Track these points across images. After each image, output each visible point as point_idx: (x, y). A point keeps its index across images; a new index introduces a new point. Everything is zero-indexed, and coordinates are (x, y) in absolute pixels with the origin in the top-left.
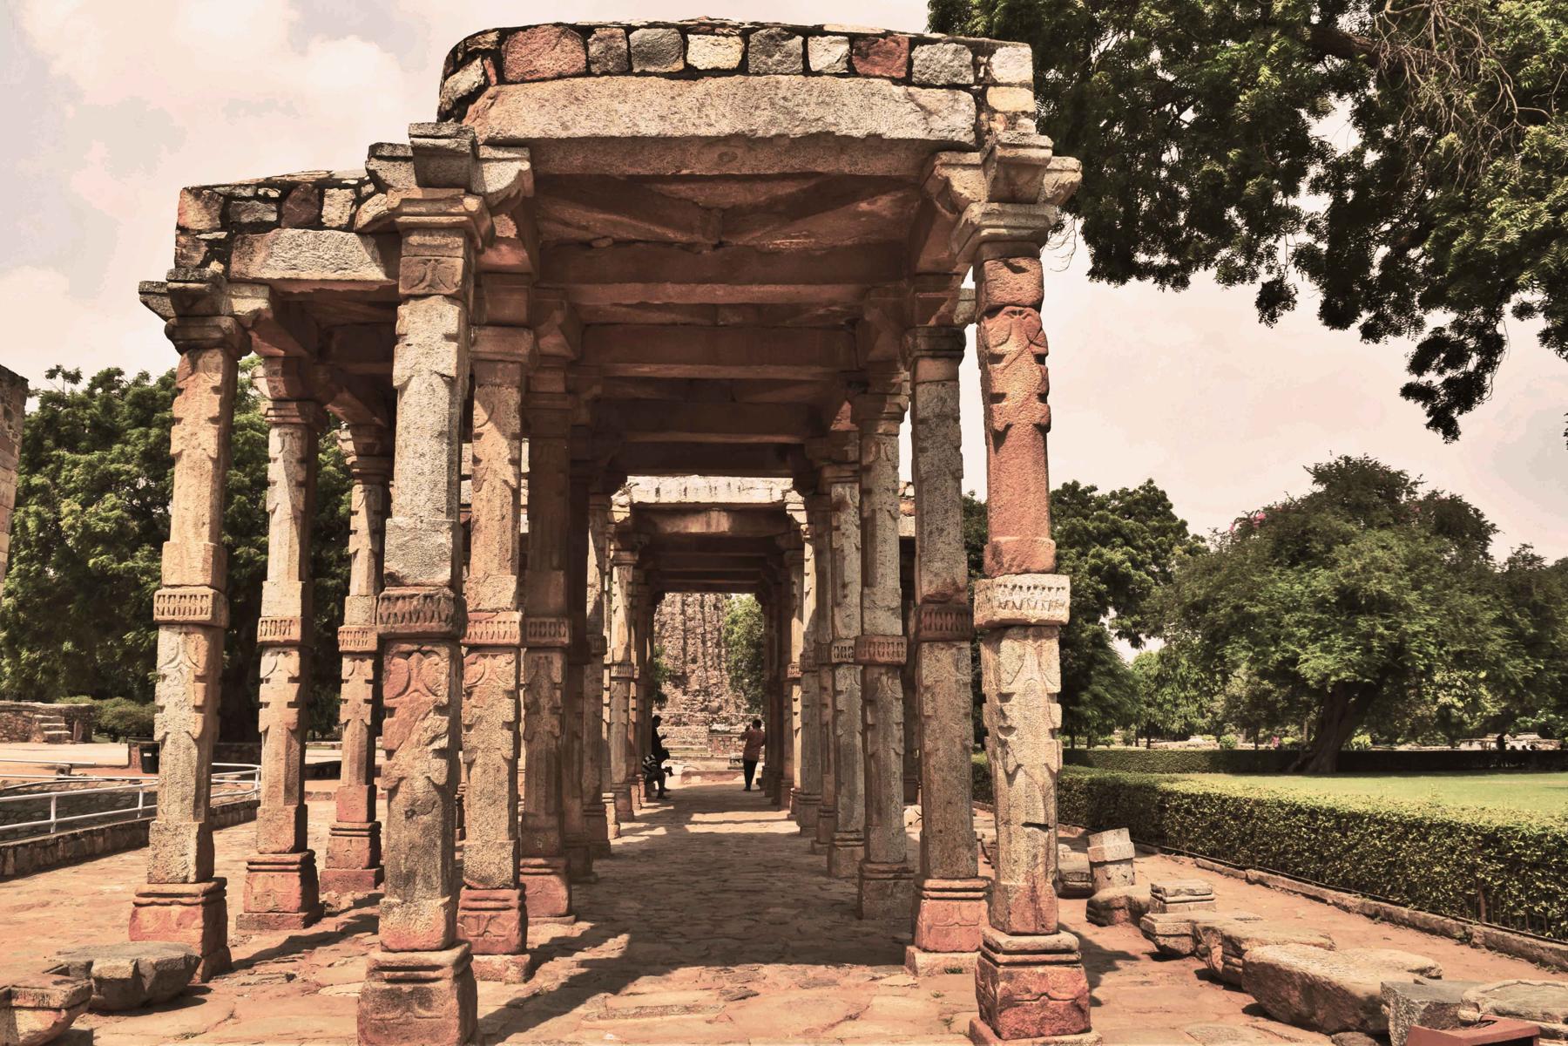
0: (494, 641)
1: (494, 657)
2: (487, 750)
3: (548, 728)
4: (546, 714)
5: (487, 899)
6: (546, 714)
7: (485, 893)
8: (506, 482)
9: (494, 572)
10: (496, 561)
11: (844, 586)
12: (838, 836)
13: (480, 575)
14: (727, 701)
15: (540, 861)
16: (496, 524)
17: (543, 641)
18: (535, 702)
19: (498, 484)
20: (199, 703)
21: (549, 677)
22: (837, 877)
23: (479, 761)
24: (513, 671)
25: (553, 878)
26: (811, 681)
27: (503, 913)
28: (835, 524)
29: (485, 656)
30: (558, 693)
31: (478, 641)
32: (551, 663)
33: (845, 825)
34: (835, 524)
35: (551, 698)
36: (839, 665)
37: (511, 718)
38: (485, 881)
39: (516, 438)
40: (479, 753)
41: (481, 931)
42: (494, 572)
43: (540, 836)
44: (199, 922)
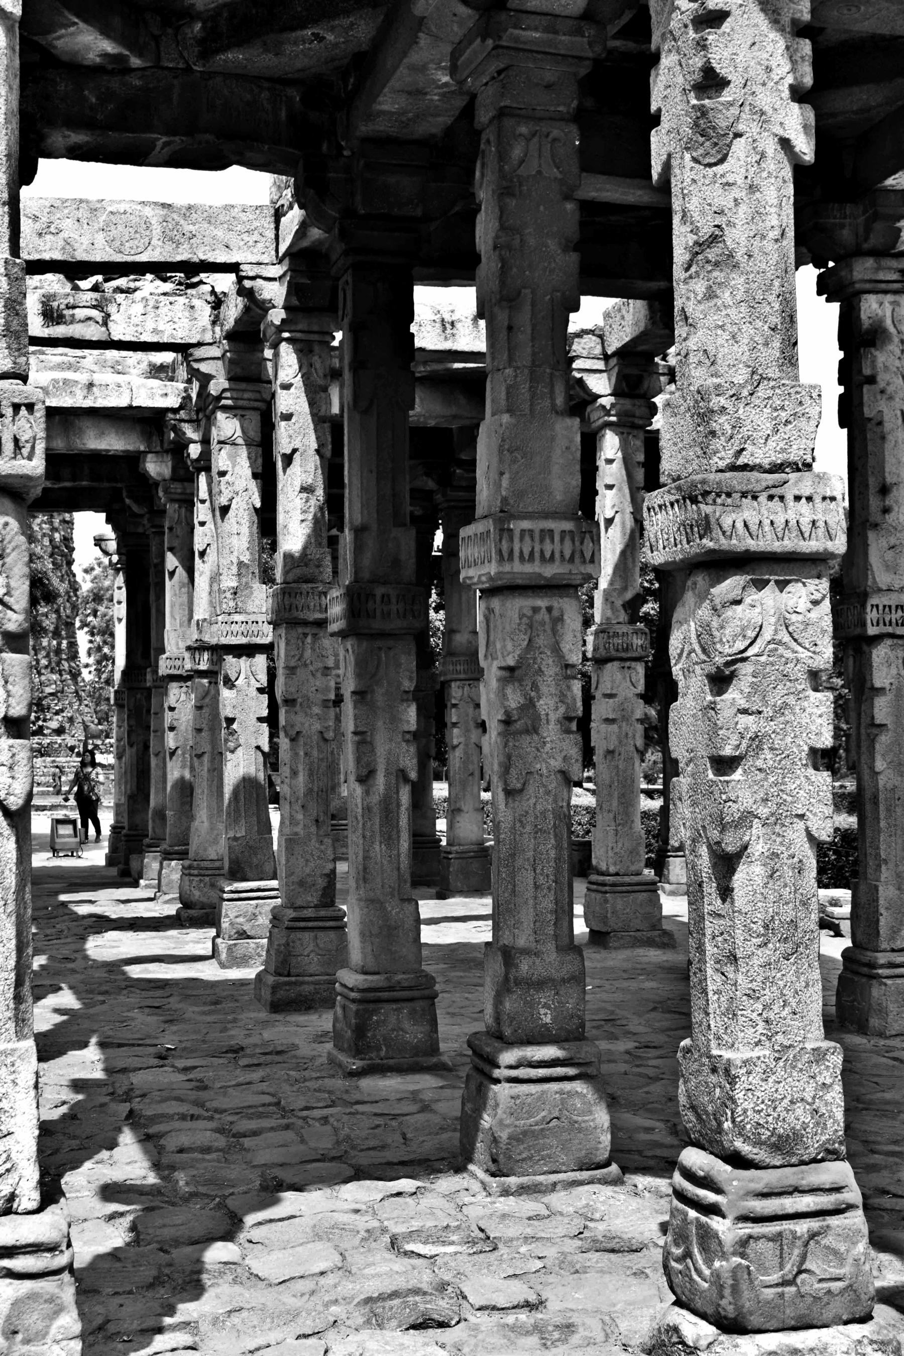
0: (789, 544)
1: (782, 585)
2: (775, 821)
3: (556, 763)
4: (551, 731)
5: (797, 1190)
6: (551, 731)
7: (789, 1176)
8: (785, 143)
9: (773, 372)
10: (777, 344)
11: (884, 490)
12: (882, 958)
13: (741, 376)
14: (71, 720)
15: (550, 1052)
16: (769, 246)
17: (549, 571)
18: (529, 705)
19: (771, 146)
20: (18, 710)
21: (557, 650)
22: (881, 1035)
23: (758, 848)
24: (827, 623)
25: (579, 1086)
26: (618, 676)
27: (834, 1221)
28: (867, 371)
29: (760, 585)
30: (577, 687)
31: (752, 545)
32: (560, 619)
33: (892, 938)
34: (867, 371)
35: (562, 698)
36: (877, 639)
37: (826, 740)
38: (784, 1145)
39: (800, 30)
40: (757, 828)
41: (790, 1268)
42: (773, 372)
43: (544, 997)
44: (69, 1321)
